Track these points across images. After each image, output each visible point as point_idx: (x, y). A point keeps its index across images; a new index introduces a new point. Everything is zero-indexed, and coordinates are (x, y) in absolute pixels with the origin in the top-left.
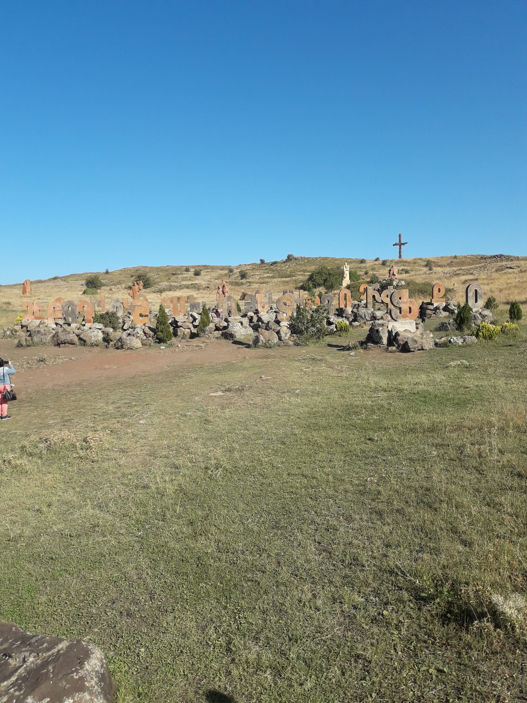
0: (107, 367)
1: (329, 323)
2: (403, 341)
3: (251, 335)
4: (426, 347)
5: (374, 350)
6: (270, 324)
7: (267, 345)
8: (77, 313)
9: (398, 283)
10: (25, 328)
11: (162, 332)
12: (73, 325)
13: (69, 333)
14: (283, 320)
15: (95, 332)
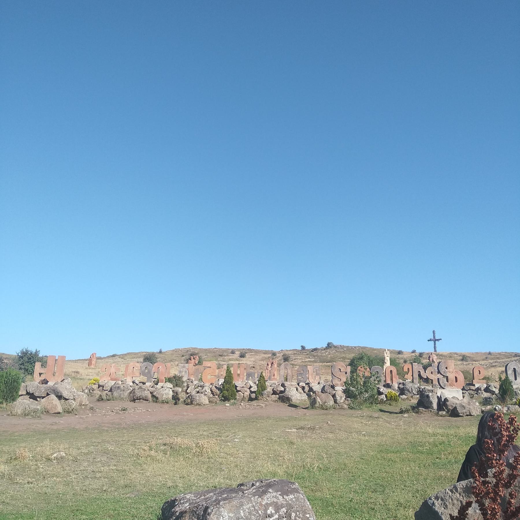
0: (185, 413)
1: (380, 393)
2: (452, 406)
3: (305, 401)
4: (474, 413)
5: (425, 415)
6: (326, 388)
7: (324, 407)
8: (152, 373)
10: (101, 388)
11: (228, 391)
12: (148, 384)
13: (145, 390)
14: (337, 385)
15: (166, 391)
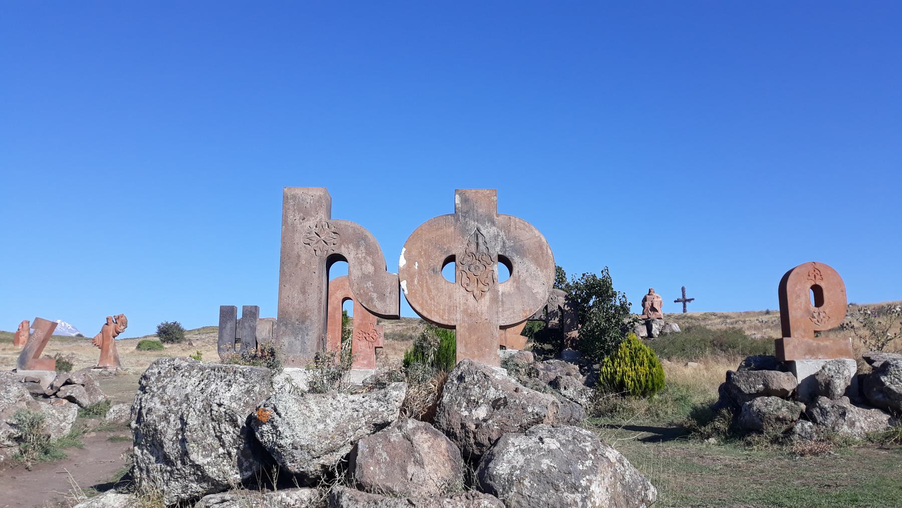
9: (664, 327)
